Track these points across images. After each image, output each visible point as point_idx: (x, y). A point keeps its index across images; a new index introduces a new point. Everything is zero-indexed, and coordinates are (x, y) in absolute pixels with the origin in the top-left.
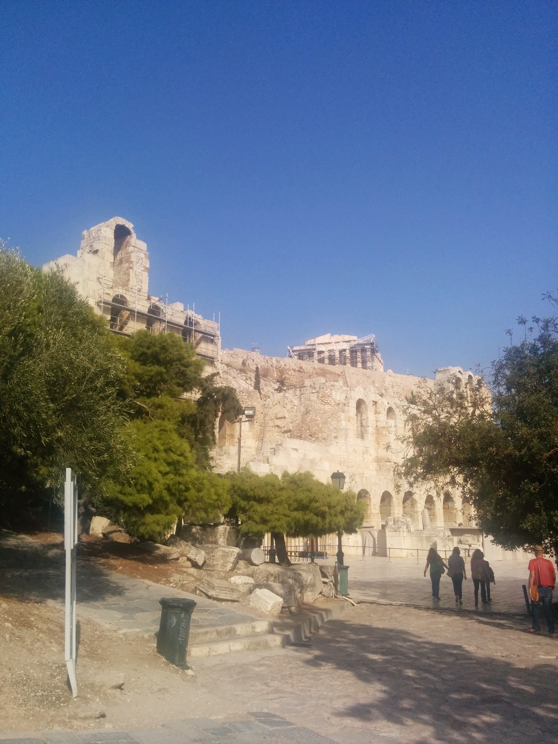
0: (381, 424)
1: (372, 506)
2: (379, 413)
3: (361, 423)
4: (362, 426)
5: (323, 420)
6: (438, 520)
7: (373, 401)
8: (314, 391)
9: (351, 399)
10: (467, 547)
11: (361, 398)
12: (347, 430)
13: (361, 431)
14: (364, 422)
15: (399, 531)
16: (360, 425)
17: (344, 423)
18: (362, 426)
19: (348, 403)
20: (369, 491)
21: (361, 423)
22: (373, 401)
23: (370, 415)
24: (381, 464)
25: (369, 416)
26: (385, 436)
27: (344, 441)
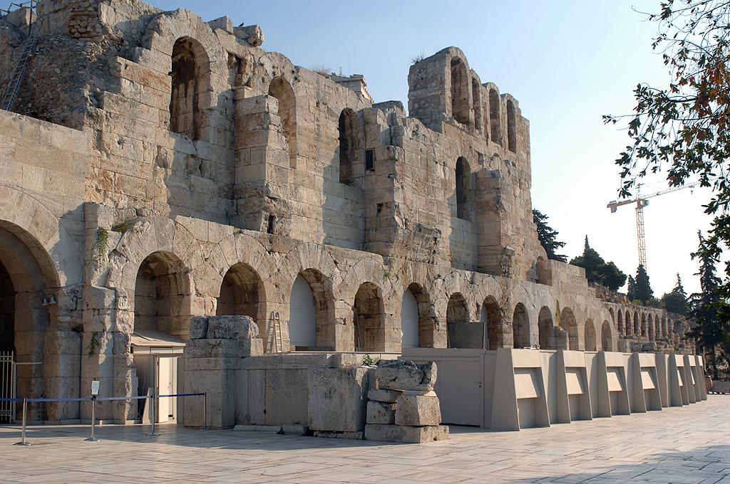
0: (245, 109)
1: (193, 296)
2: (248, 84)
3: (195, 103)
4: (196, 109)
5: (66, 74)
6: (387, 337)
7: (230, 54)
8: (57, 8)
9: (160, 32)
10: (386, 396)
11: (192, 34)
12: (134, 103)
13: (195, 122)
14: (201, 98)
15: (216, 355)
16: (191, 107)
17: (125, 84)
18: (196, 109)
19: (149, 40)
20: (183, 258)
21: (195, 103)
22: (230, 54)
23: (219, 82)
24: (241, 202)
25: (214, 84)
26: (253, 134)
27: (123, 132)
